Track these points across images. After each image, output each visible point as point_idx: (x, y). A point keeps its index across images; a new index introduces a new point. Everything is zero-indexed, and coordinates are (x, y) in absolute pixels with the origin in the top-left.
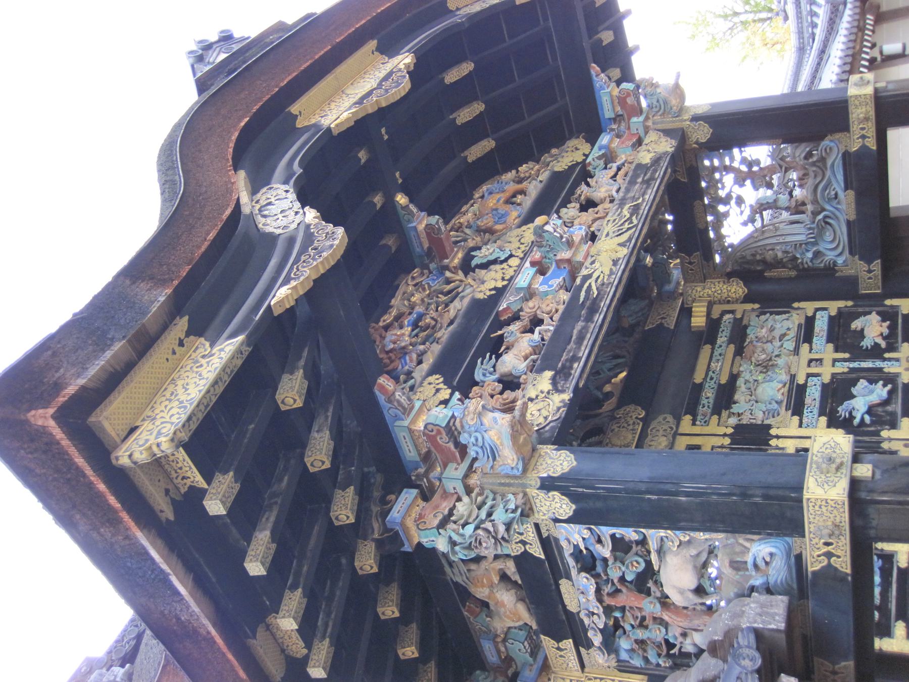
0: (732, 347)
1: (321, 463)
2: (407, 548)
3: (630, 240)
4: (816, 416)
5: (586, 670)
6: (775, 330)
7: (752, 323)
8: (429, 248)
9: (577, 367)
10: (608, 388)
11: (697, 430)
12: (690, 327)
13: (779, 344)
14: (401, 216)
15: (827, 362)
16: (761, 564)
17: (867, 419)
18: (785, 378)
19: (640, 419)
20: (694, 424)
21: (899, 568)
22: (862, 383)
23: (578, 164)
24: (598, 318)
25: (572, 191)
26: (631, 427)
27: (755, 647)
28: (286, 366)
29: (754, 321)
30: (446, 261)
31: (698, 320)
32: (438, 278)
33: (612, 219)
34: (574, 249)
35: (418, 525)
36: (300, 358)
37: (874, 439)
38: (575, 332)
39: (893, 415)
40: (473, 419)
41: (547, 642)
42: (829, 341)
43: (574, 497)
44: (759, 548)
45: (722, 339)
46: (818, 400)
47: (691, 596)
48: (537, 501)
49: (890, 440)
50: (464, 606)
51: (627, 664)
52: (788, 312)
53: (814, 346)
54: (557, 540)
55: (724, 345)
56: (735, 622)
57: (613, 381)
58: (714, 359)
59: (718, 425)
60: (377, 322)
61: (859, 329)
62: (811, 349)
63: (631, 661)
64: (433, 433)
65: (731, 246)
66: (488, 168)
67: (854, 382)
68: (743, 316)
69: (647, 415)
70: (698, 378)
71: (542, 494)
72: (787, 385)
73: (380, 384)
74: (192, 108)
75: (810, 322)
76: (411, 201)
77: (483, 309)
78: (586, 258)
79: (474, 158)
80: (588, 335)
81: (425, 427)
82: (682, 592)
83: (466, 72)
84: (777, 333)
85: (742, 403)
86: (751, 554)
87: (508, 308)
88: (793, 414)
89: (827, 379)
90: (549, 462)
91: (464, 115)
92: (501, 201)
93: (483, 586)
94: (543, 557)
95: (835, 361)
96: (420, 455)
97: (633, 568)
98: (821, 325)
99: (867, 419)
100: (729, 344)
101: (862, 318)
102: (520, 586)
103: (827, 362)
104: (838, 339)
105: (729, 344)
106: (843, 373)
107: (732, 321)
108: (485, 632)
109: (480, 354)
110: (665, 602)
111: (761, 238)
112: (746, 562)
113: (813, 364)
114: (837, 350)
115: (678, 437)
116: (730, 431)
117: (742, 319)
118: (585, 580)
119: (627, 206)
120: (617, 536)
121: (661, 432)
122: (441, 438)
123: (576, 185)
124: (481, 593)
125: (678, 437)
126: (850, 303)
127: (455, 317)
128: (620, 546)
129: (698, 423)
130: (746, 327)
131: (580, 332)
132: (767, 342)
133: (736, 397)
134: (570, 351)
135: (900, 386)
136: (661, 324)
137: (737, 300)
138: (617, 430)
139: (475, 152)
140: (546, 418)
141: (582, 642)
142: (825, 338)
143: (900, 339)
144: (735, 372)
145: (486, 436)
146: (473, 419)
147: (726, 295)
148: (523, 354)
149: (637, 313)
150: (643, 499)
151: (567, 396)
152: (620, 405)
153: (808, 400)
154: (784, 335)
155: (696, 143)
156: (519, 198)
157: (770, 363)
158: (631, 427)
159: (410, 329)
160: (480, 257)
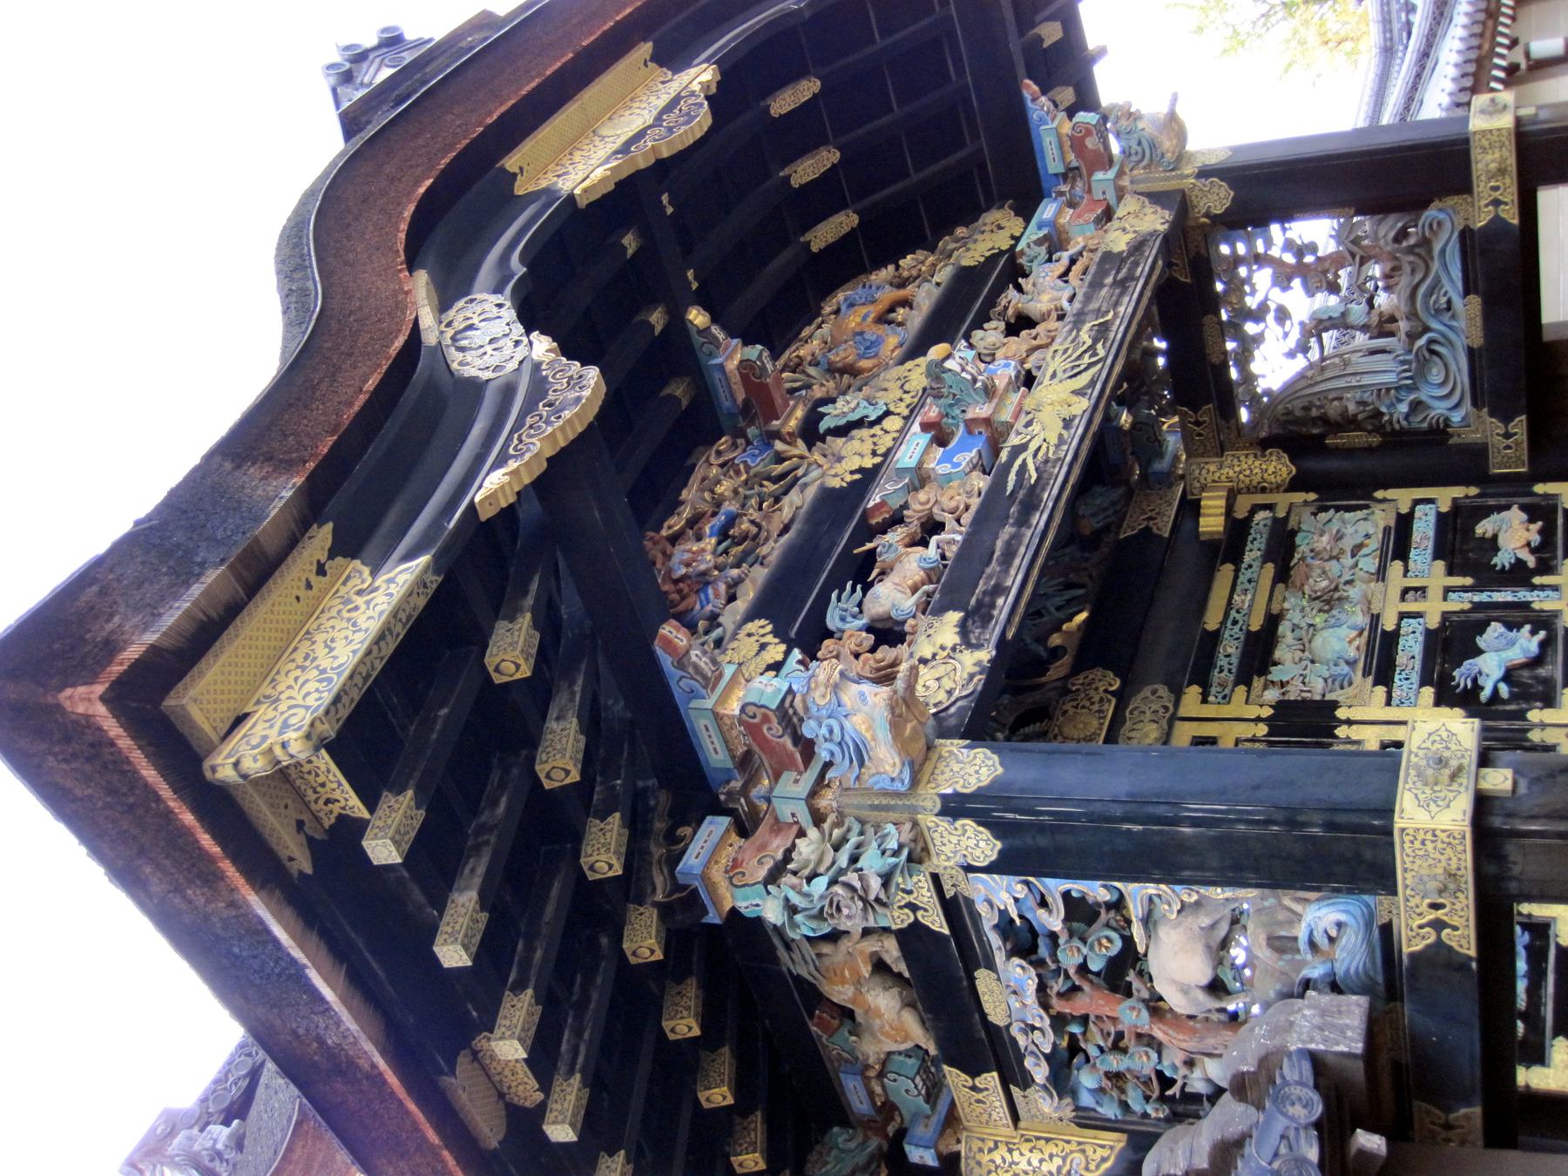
0: (1270, 567)
1: (563, 774)
2: (713, 918)
3: (1092, 383)
4: (1415, 686)
5: (1022, 1124)
6: (1344, 538)
7: (1304, 527)
8: (746, 402)
9: (1003, 604)
10: (1055, 640)
12: (1197, 533)
13: (1350, 562)
14: (697, 346)
15: (1435, 592)
16: (1322, 942)
17: (1504, 690)
18: (1361, 620)
19: (1112, 693)
20: (1204, 701)
21: (1558, 946)
22: (1496, 629)
23: (1002, 253)
24: (1039, 519)
26: (1096, 707)
27: (1311, 1083)
28: (501, 606)
29: (1307, 521)
30: (776, 423)
31: (1212, 522)
32: (761, 453)
33: (1062, 348)
34: (995, 401)
35: (731, 878)
36: (525, 593)
37: (1517, 724)
38: (999, 544)
39: (1548, 683)
40: (824, 696)
41: (955, 1078)
42: (1437, 556)
43: (998, 829)
44: (1318, 914)
45: (1252, 554)
46: (1419, 657)
47: (1201, 996)
48: (936, 835)
49: (1543, 726)
50: (811, 1016)
51: (1092, 1114)
52: (1367, 507)
53: (1411, 565)
54: (970, 903)
55: (1256, 564)
56: (1277, 1042)
57: (1065, 627)
58: (1239, 589)
59: (1247, 702)
60: (658, 529)
61: (1489, 535)
62: (1406, 571)
63: (1099, 1109)
64: (755, 721)
65: (1268, 392)
66: (845, 264)
67: (1481, 627)
68: (1288, 513)
69: (1124, 684)
70: (1212, 621)
71: (944, 823)
72: (1366, 634)
73: (664, 638)
74: (333, 163)
75: (1404, 523)
76: (714, 320)
77: (840, 504)
78: (1017, 416)
79: (823, 245)
80: (1022, 550)
81: (743, 710)
82: (1185, 990)
83: (807, 96)
84: (1347, 544)
85: (1288, 663)
86: (1304, 925)
87: (883, 504)
88: (1375, 684)
89: (1434, 622)
90: (956, 768)
91: (805, 171)
92: (870, 319)
93: (843, 982)
94: (946, 931)
95: (1448, 590)
96: (733, 757)
97: (1102, 949)
98: (1424, 529)
99: (1504, 690)
100: (1265, 562)
101: (1495, 517)
102: (907, 981)
103: (1435, 592)
104: (1452, 552)
105: (1265, 562)
106: (1462, 612)
107: (1269, 522)
108: (847, 1061)
109: (836, 582)
110: (1155, 1006)
111: (1319, 379)
112: (1295, 939)
113: (1411, 595)
114: (1451, 572)
115: (1178, 724)
116: (1267, 712)
117: (1286, 519)
118: (1018, 970)
119: (1088, 326)
120: (1074, 894)
121: (1148, 715)
122: (770, 729)
123: (998, 290)
124: (841, 993)
125: (1178, 725)
126: (1473, 491)
127: (792, 521)
128: (1080, 912)
129: (1211, 698)
130: (1294, 533)
131: (1008, 544)
132: (1331, 558)
133: (1278, 654)
134: (990, 577)
135: (1561, 633)
136: (1148, 529)
137: (1278, 487)
138: (1071, 712)
139: (824, 235)
140: (950, 693)
141: (1013, 1076)
143: (1560, 552)
144: (1275, 611)
145: (847, 724)
146: (824, 696)
147: (1258, 478)
148: (910, 582)
149: (1105, 509)
150: (1119, 832)
151: (985, 655)
152: (1076, 669)
153: (1401, 659)
154: (1359, 547)
155: (1207, 215)
156: (901, 313)
157: (1337, 595)
158: (1096, 707)
159: (713, 541)
160: (834, 415)
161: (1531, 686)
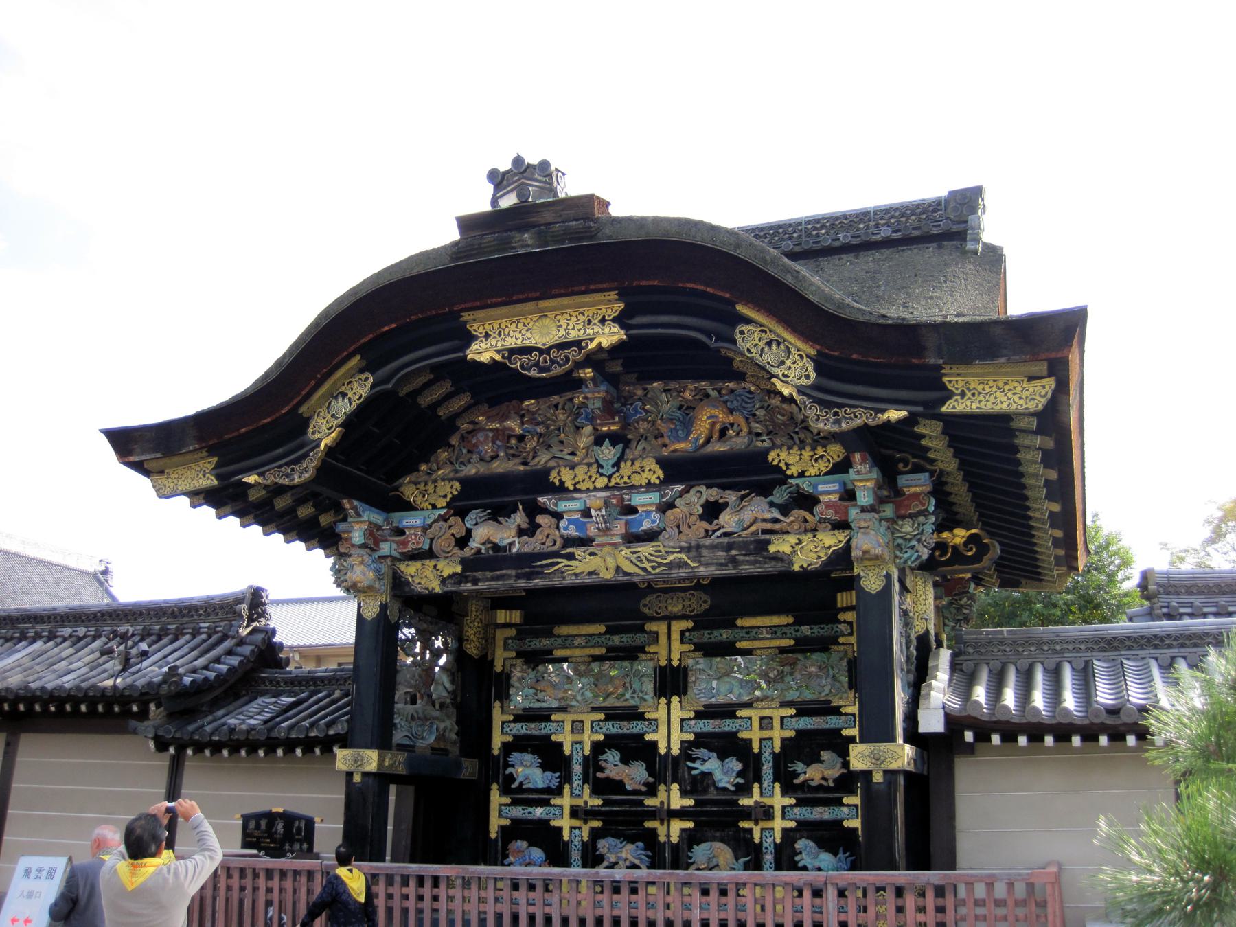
3: (629, 574)
11: (676, 636)
24: (522, 583)
25: (724, 487)
33: (661, 548)
37: (669, 779)
38: (504, 572)
39: (705, 791)
42: (799, 732)
45: (805, 630)
49: (668, 791)
55: (799, 634)
77: (541, 482)
78: (599, 545)
88: (695, 712)
89: (743, 735)
99: (694, 772)
116: (675, 663)
129: (687, 634)
142: (809, 727)
151: (438, 590)
153: (716, 722)
161: (702, 783)
